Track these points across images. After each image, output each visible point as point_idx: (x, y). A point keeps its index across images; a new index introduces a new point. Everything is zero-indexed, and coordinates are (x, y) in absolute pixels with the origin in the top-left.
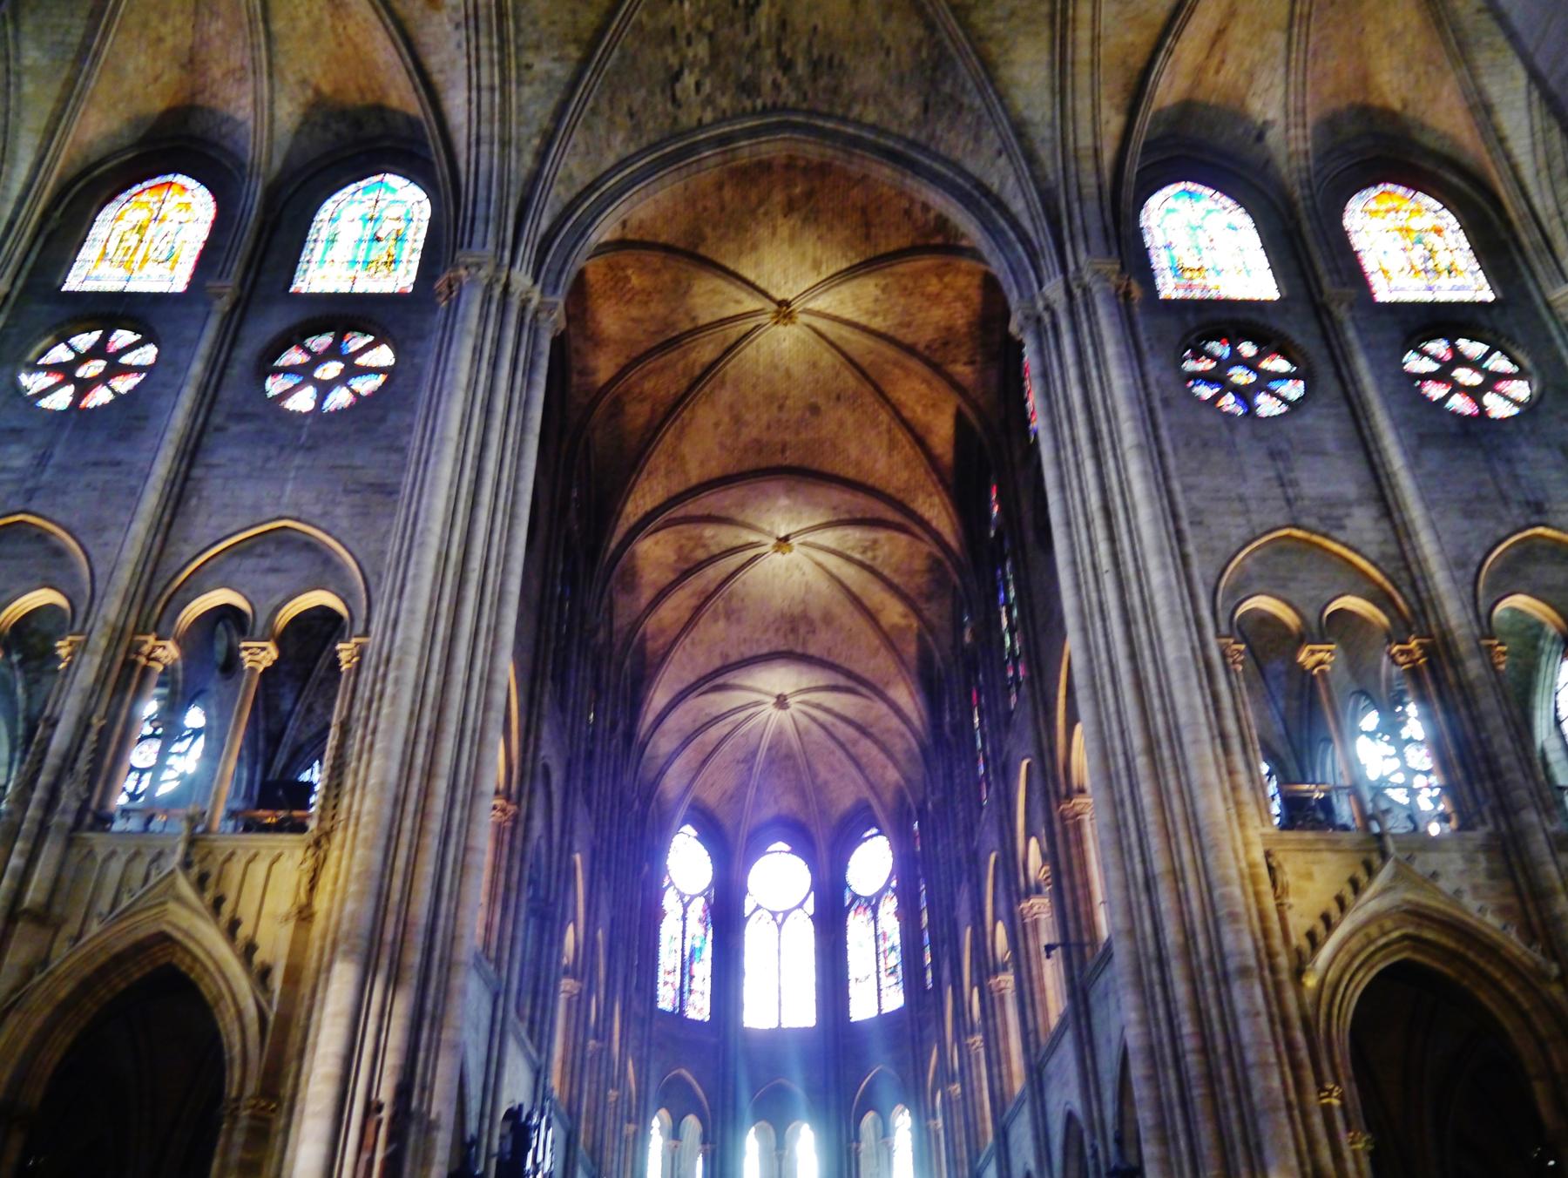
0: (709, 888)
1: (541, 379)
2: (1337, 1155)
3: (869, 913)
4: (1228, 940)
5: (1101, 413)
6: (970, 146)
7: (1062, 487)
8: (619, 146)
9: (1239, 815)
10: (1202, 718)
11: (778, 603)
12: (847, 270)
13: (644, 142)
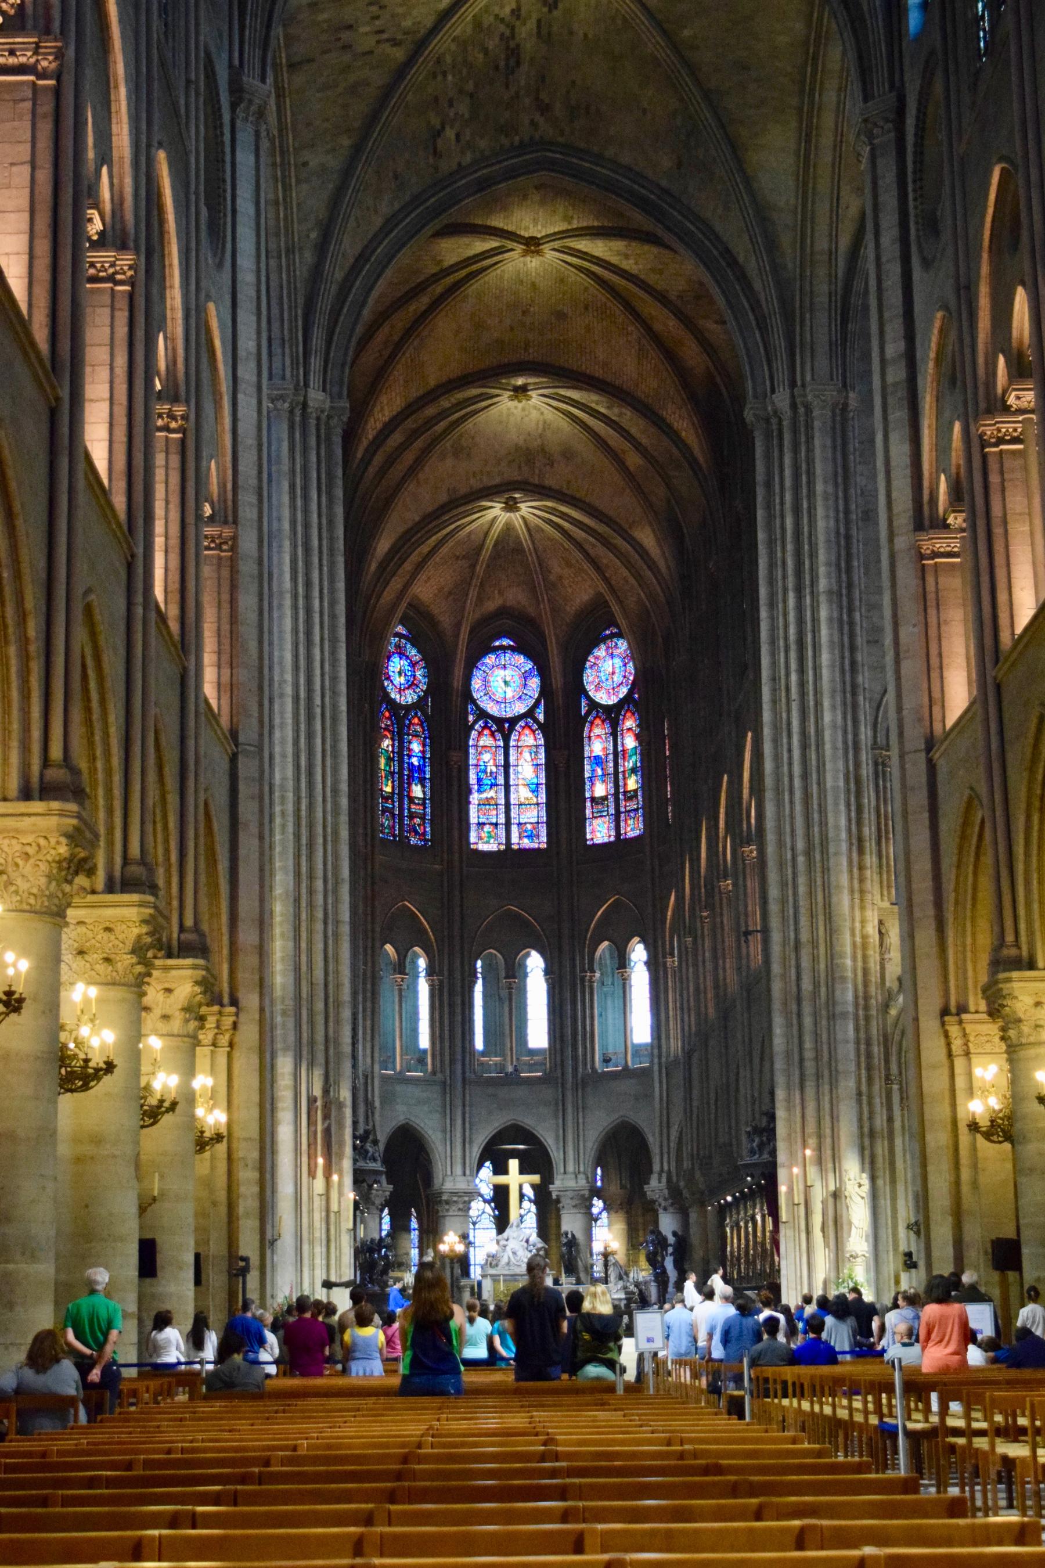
0: (426, 692)
1: (339, 493)
2: (890, 1119)
3: (607, 726)
4: (838, 993)
5: (806, 547)
6: (720, 211)
7: (772, 605)
8: (386, 207)
9: (862, 900)
10: (844, 835)
11: (513, 437)
12: (598, 228)
13: (407, 198)
